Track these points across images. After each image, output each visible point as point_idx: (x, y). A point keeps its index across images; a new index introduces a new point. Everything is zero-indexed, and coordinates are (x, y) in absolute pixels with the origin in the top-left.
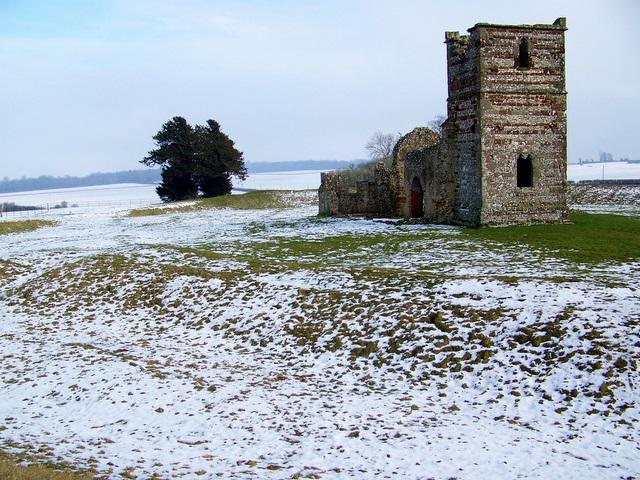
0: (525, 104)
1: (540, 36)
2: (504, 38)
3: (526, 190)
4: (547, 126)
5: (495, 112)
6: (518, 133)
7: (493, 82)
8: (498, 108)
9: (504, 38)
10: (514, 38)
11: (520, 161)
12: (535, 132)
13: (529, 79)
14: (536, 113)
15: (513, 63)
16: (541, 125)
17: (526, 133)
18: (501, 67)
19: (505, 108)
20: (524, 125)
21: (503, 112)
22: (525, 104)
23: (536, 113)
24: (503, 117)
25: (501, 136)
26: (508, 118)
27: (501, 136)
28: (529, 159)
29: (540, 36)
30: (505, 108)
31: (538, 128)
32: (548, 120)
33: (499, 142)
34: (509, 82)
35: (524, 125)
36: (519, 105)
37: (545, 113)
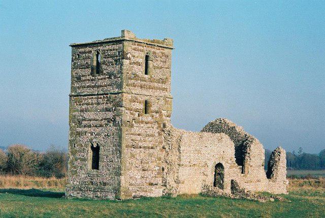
0: (95, 104)
1: (107, 48)
2: (85, 53)
3: (95, 172)
4: (109, 120)
5: (77, 111)
6: (90, 126)
7: (78, 88)
8: (79, 108)
9: (85, 53)
10: (91, 51)
11: (92, 147)
12: (101, 126)
13: (99, 83)
14: (102, 110)
15: (89, 71)
16: (105, 119)
17: (96, 126)
18: (83, 76)
19: (84, 107)
20: (94, 120)
21: (82, 111)
22: (95, 104)
23: (102, 110)
24: (82, 114)
25: (79, 130)
26: (86, 115)
27: (79, 130)
28: (98, 147)
29: (107, 48)
30: (84, 107)
31: (103, 122)
32: (110, 115)
33: (79, 134)
34: (88, 87)
35: (94, 120)
36: (92, 104)
37: (107, 110)
